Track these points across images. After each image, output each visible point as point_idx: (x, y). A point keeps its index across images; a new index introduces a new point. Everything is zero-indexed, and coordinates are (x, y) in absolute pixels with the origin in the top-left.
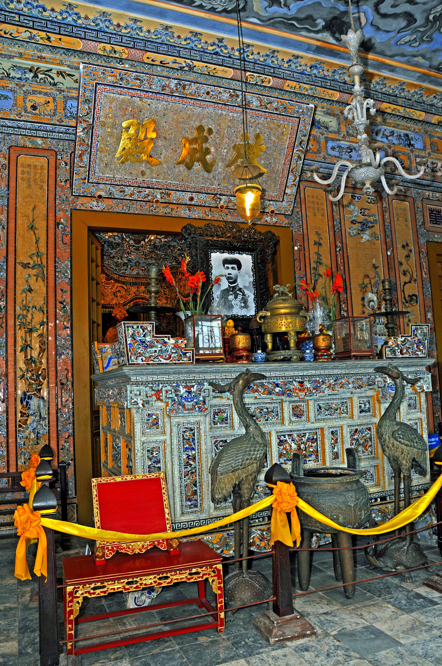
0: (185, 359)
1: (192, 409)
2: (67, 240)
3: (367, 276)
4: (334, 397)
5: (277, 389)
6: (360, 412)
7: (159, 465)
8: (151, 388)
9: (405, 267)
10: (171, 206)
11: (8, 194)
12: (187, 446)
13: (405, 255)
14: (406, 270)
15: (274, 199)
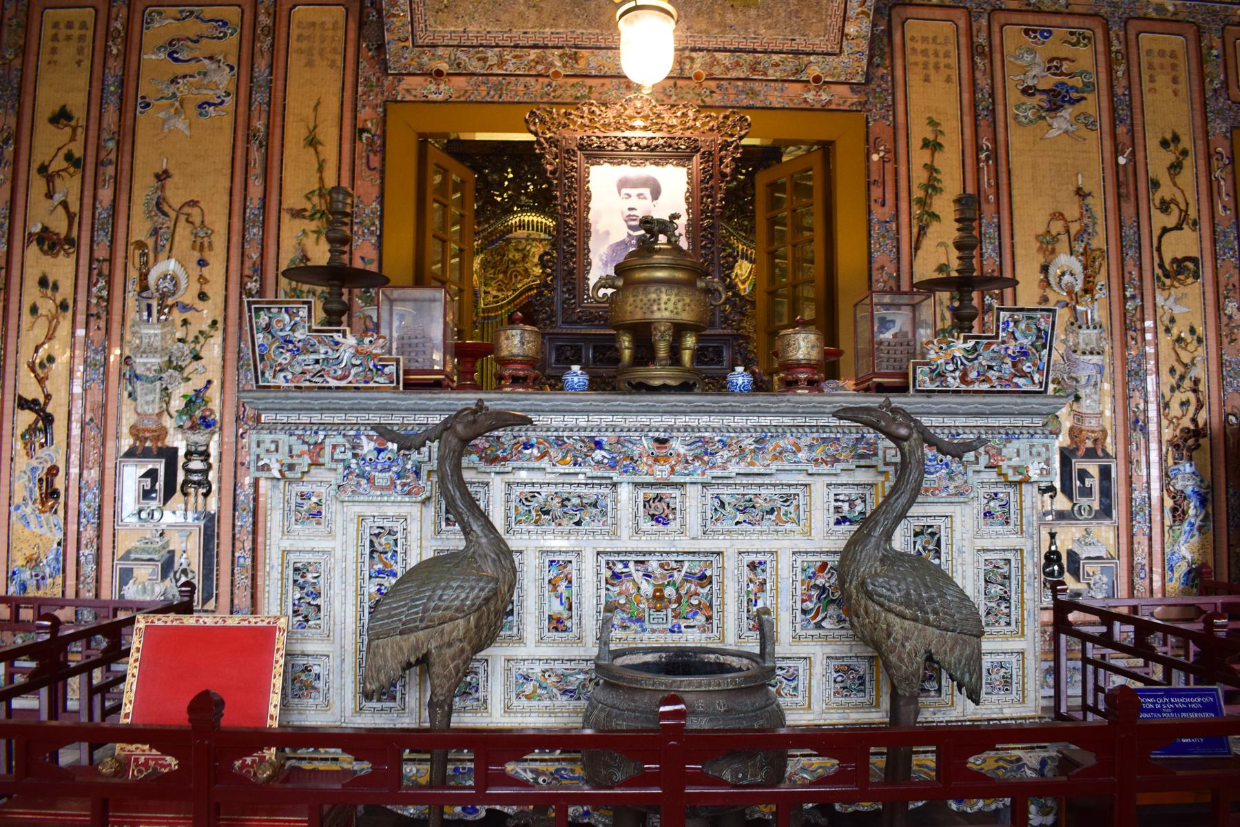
0: (381, 380)
1: (387, 488)
2: (375, 161)
3: (1059, 216)
4: (759, 480)
5: (598, 455)
6: (838, 522)
7: (318, 602)
8: (299, 437)
9: (1166, 191)
10: (589, 82)
11: (271, 81)
12: (380, 566)
13: (1168, 163)
14: (1167, 198)
15: (819, 50)
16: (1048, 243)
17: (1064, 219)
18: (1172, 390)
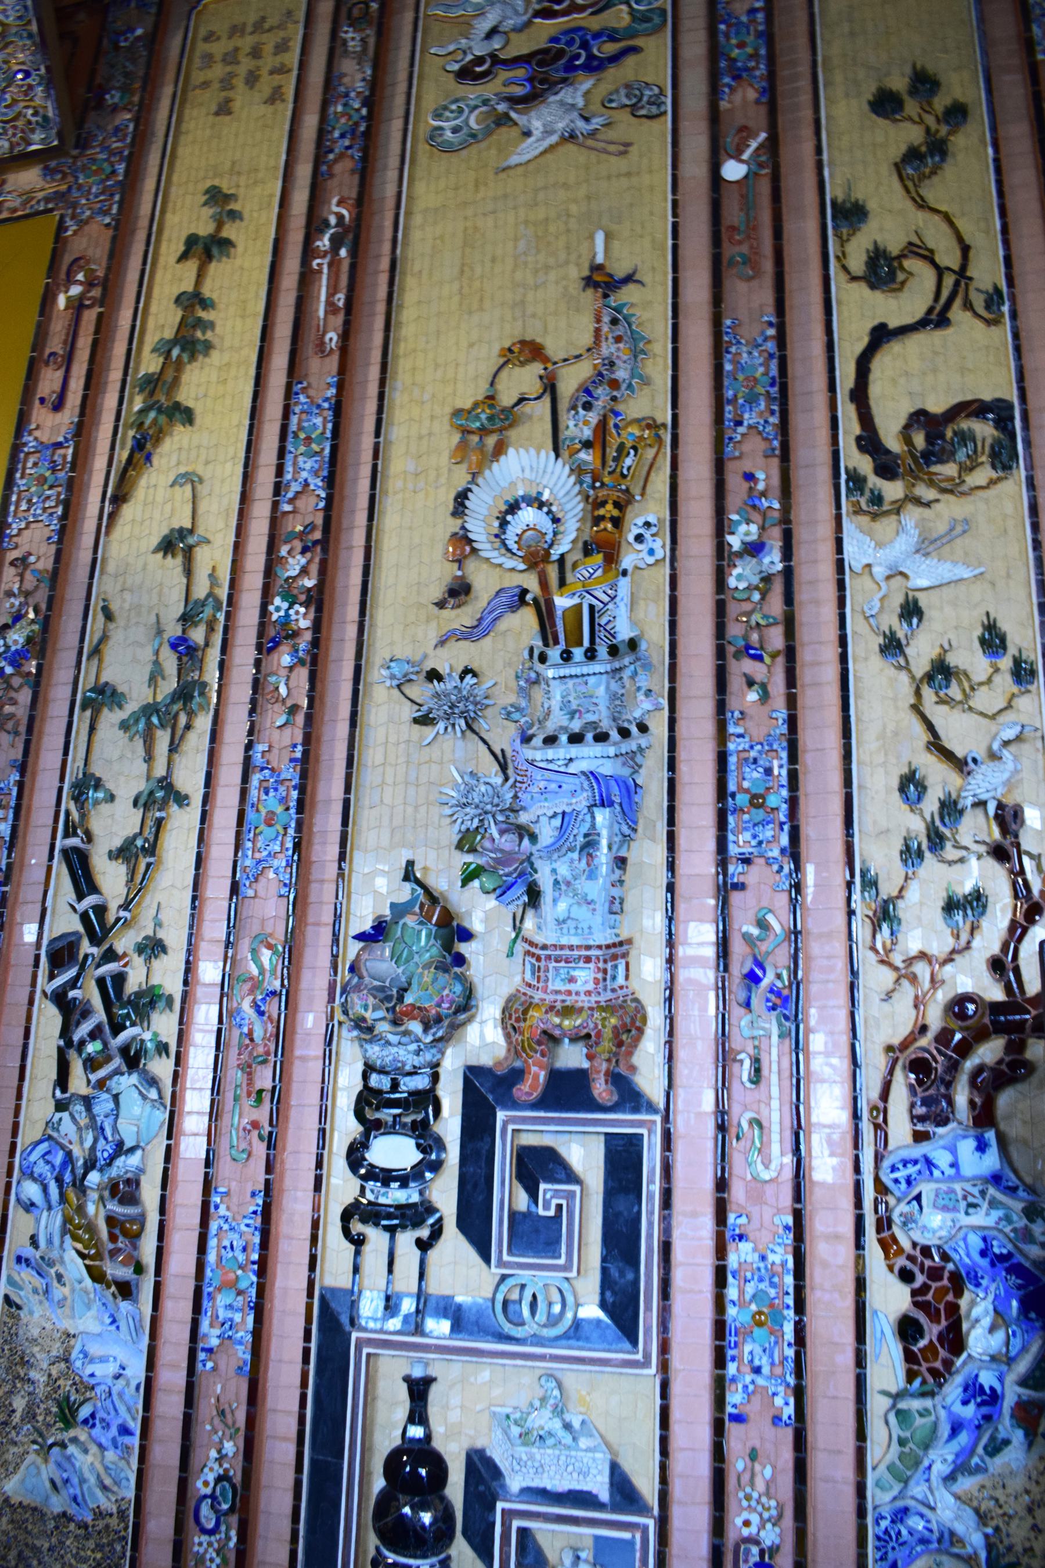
13: (897, 150)
16: (483, 431)
17: (546, 360)
18: (911, 855)
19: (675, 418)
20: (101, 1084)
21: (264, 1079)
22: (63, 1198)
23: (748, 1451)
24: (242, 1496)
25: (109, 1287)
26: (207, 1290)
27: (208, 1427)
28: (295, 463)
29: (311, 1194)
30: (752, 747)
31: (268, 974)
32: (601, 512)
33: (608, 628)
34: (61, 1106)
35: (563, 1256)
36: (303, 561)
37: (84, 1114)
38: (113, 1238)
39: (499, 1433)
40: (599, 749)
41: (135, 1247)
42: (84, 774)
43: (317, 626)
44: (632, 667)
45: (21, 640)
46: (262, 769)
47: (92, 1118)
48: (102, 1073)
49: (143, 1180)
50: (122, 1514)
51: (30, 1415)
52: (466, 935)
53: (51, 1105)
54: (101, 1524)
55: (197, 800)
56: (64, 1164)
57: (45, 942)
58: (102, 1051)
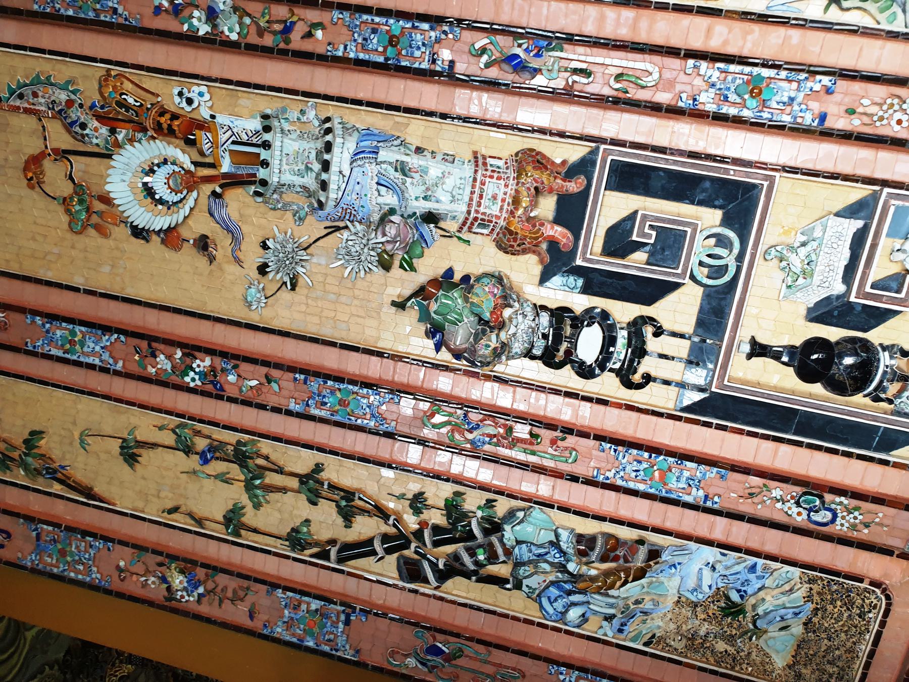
17: (43, 155)
19: (103, 61)
20: (508, 552)
21: (522, 431)
22: (582, 592)
23: (848, 116)
24: (813, 488)
25: (650, 566)
26: (664, 494)
27: (759, 507)
28: (87, 355)
29: (608, 408)
30: (355, 40)
31: (452, 419)
32: (165, 126)
33: (250, 135)
34: (518, 586)
35: (686, 229)
36: (162, 357)
37: (527, 568)
38: (616, 559)
39: (799, 294)
40: (336, 150)
41: (625, 543)
42: (286, 540)
43: (211, 352)
44: (282, 121)
45: (181, 578)
46: (308, 405)
47: (530, 562)
48: (500, 551)
49: (580, 530)
50: (811, 581)
51: (730, 640)
52: (449, 273)
53: (516, 592)
54: (816, 598)
55: (320, 457)
56: (560, 588)
57: (401, 584)
58: (484, 549)
